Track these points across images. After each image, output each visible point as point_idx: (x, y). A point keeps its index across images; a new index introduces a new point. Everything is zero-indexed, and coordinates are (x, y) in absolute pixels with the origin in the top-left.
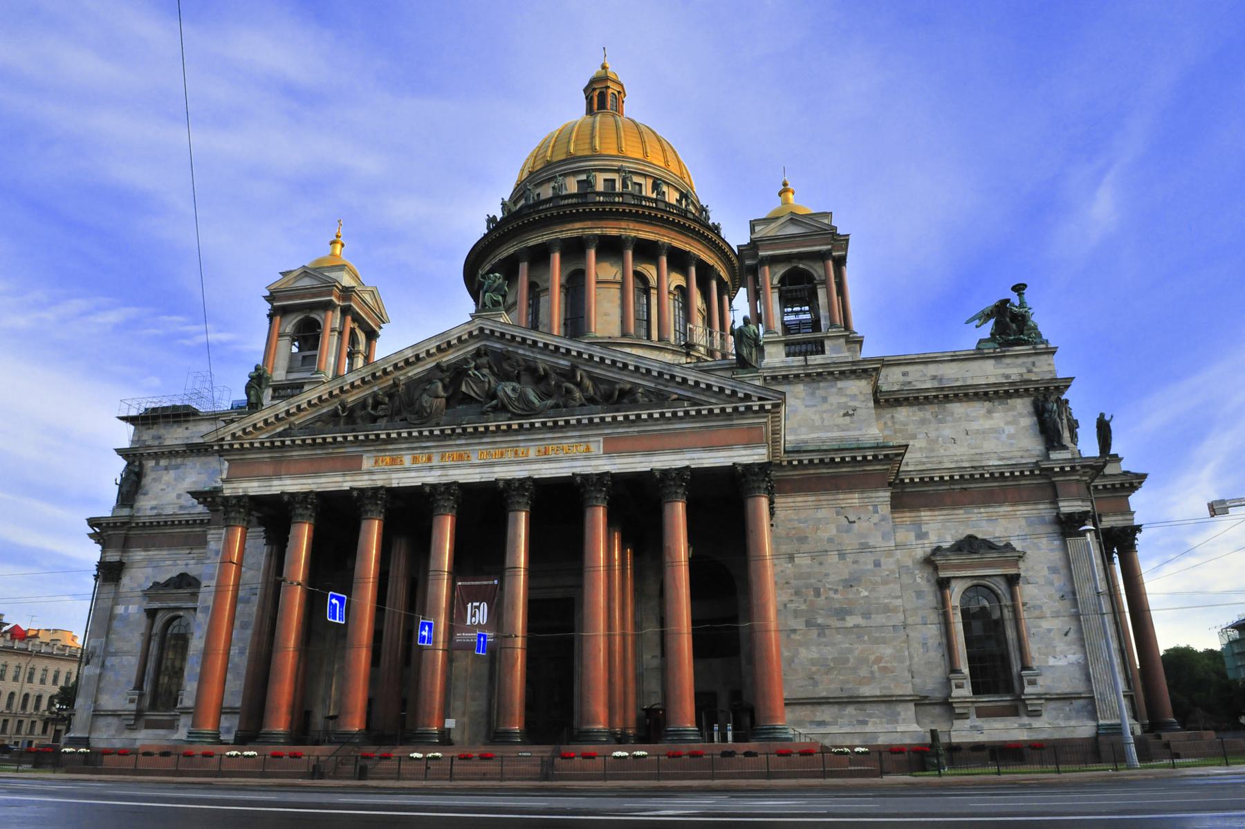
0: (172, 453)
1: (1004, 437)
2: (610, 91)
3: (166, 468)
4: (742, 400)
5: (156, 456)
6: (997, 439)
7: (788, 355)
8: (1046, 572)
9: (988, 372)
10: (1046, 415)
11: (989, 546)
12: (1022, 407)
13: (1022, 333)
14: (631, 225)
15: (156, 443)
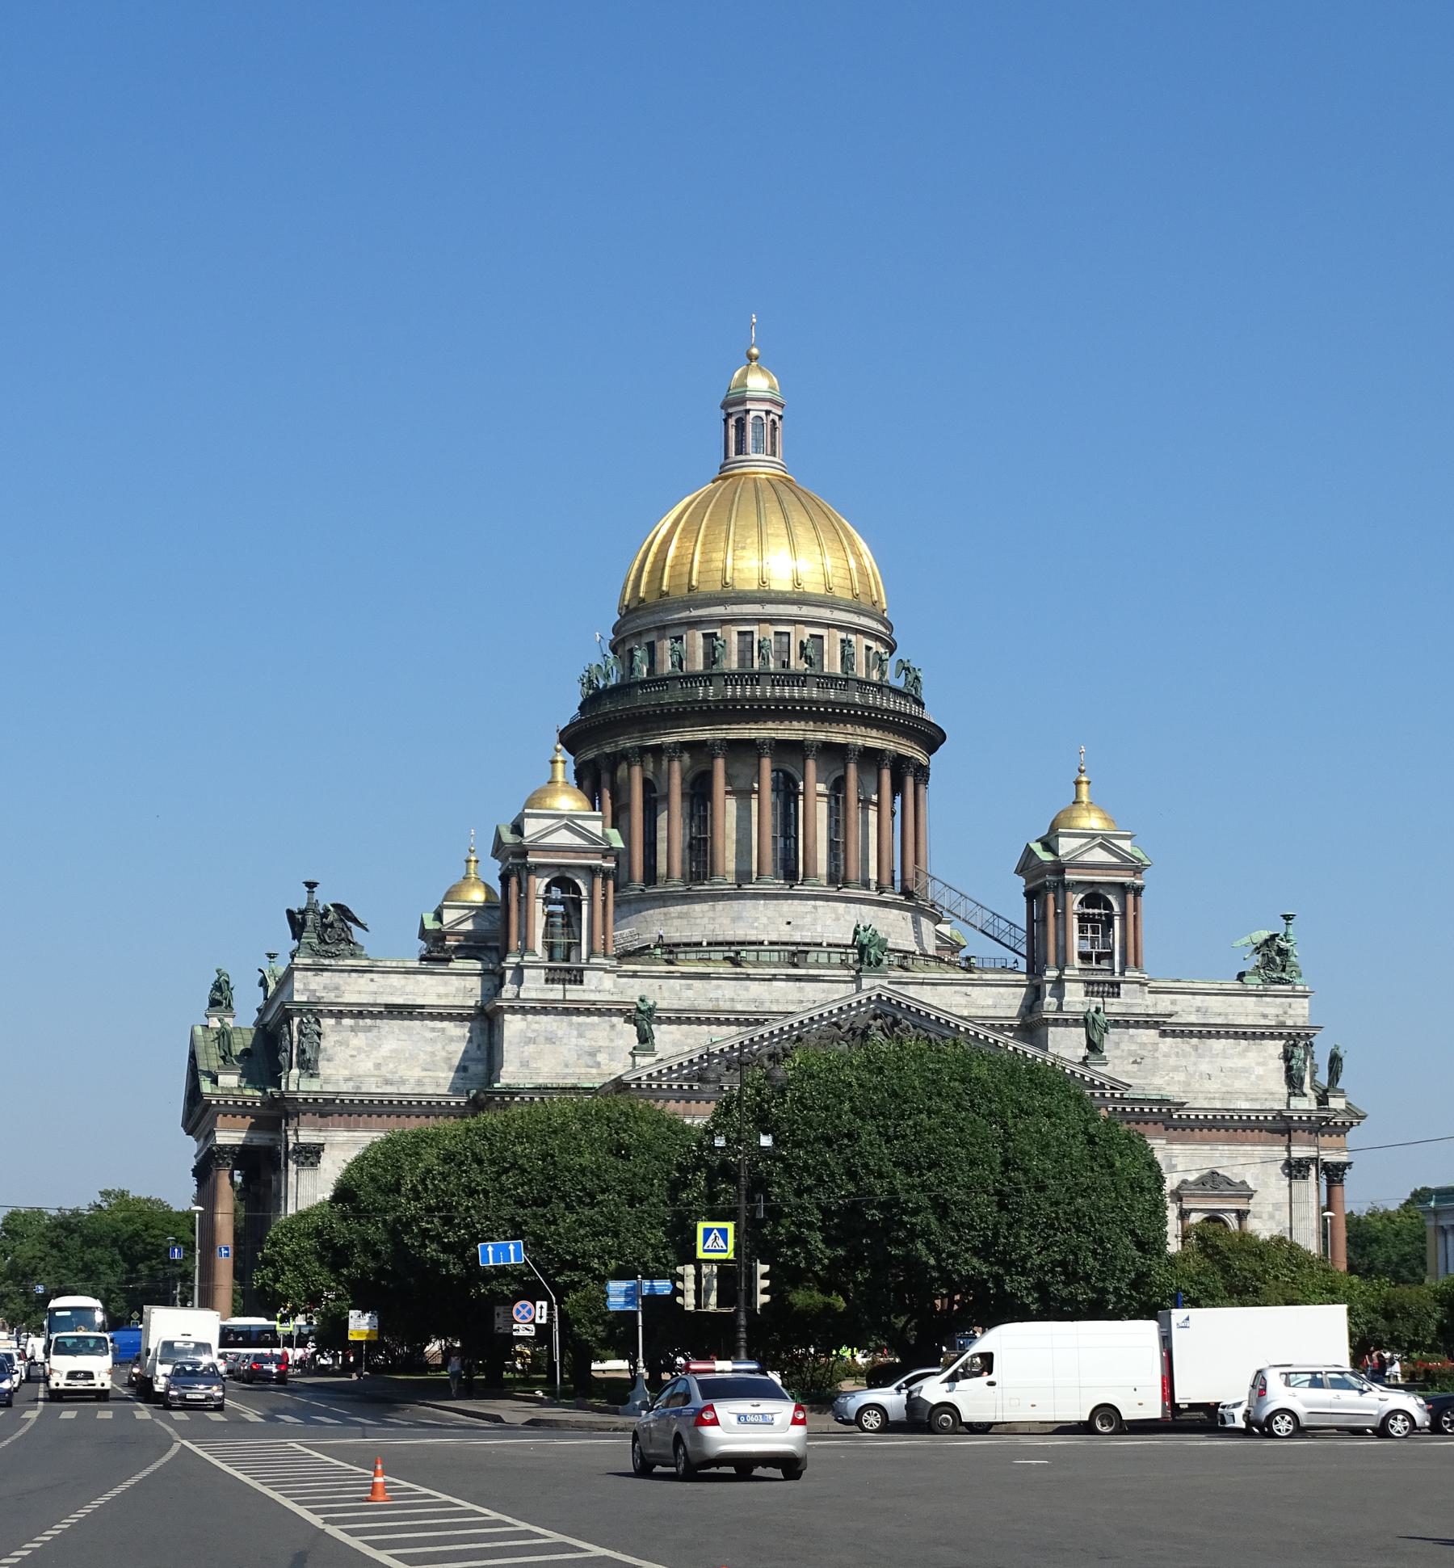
0: (360, 1013)
1: (1253, 1078)
2: (772, 416)
3: (352, 1029)
4: (1094, 1087)
5: (340, 1015)
6: (1248, 1078)
7: (1087, 994)
8: (1270, 1208)
9: (1247, 1011)
10: (1293, 1062)
11: (1230, 1183)
12: (1276, 1047)
13: (1283, 970)
14: (858, 731)
15: (330, 997)
